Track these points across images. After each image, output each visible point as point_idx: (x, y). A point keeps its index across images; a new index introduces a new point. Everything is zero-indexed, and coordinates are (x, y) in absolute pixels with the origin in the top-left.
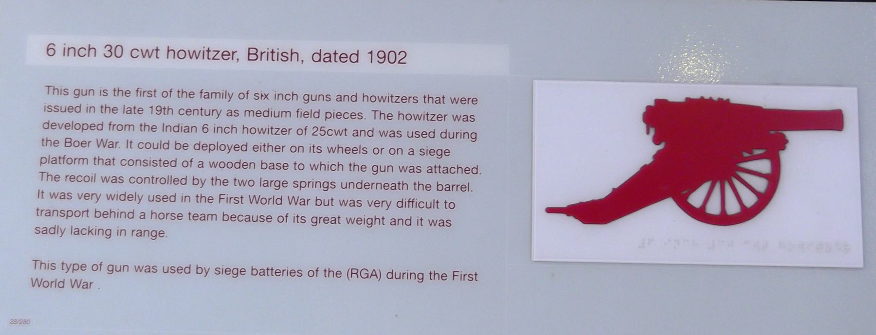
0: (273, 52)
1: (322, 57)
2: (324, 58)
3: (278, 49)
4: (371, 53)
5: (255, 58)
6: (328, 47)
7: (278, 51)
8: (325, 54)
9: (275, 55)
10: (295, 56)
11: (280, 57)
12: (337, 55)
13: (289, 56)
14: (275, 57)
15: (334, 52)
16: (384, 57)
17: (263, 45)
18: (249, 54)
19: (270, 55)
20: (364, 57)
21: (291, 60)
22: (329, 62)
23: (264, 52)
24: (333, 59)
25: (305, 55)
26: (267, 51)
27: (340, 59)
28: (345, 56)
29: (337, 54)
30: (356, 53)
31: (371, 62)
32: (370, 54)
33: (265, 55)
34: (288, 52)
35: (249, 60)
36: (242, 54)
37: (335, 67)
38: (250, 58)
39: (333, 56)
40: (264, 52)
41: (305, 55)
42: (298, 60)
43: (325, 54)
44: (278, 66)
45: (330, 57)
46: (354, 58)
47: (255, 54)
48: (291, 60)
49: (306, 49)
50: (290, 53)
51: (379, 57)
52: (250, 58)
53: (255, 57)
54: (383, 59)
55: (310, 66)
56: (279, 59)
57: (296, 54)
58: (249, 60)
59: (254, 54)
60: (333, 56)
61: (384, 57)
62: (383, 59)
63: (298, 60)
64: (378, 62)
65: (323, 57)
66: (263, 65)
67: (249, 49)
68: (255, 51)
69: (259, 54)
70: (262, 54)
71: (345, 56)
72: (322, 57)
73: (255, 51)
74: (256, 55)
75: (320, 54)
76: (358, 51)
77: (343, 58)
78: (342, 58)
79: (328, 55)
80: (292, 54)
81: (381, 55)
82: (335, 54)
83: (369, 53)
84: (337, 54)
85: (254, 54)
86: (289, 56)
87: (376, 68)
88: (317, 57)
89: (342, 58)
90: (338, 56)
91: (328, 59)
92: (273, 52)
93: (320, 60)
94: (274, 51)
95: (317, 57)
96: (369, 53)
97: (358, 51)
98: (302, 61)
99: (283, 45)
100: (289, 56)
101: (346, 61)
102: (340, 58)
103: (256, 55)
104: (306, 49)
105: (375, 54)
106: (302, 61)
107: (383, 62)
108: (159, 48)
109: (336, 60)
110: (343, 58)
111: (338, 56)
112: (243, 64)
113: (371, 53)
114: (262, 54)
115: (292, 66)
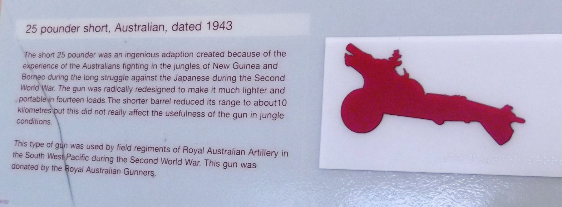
4: (209, 23)
7: (151, 24)
12: (188, 26)
16: (217, 26)
20: (205, 26)
24: (185, 29)
25: (168, 27)
27: (189, 28)
29: (188, 25)
32: (209, 24)
37: (187, 34)
39: (185, 26)
41: (168, 27)
42: (163, 30)
43: (180, 26)
45: (183, 27)
46: (198, 27)
49: (169, 22)
54: (217, 27)
55: (170, 34)
60: (185, 26)
61: (217, 26)
62: (217, 27)
63: (163, 30)
65: (179, 27)
75: (177, 26)
77: (192, 27)
78: (191, 27)
79: (182, 26)
81: (216, 24)
82: (187, 25)
83: (208, 23)
84: (188, 25)
88: (175, 28)
89: (191, 27)
90: (188, 26)
96: (208, 23)
98: (166, 30)
102: (190, 27)
104: (169, 22)
105: (211, 24)
106: (166, 30)
107: (217, 29)
108: (107, 25)
109: (187, 29)
110: (192, 27)
111: (188, 26)
113: (209, 23)
115: (160, 34)
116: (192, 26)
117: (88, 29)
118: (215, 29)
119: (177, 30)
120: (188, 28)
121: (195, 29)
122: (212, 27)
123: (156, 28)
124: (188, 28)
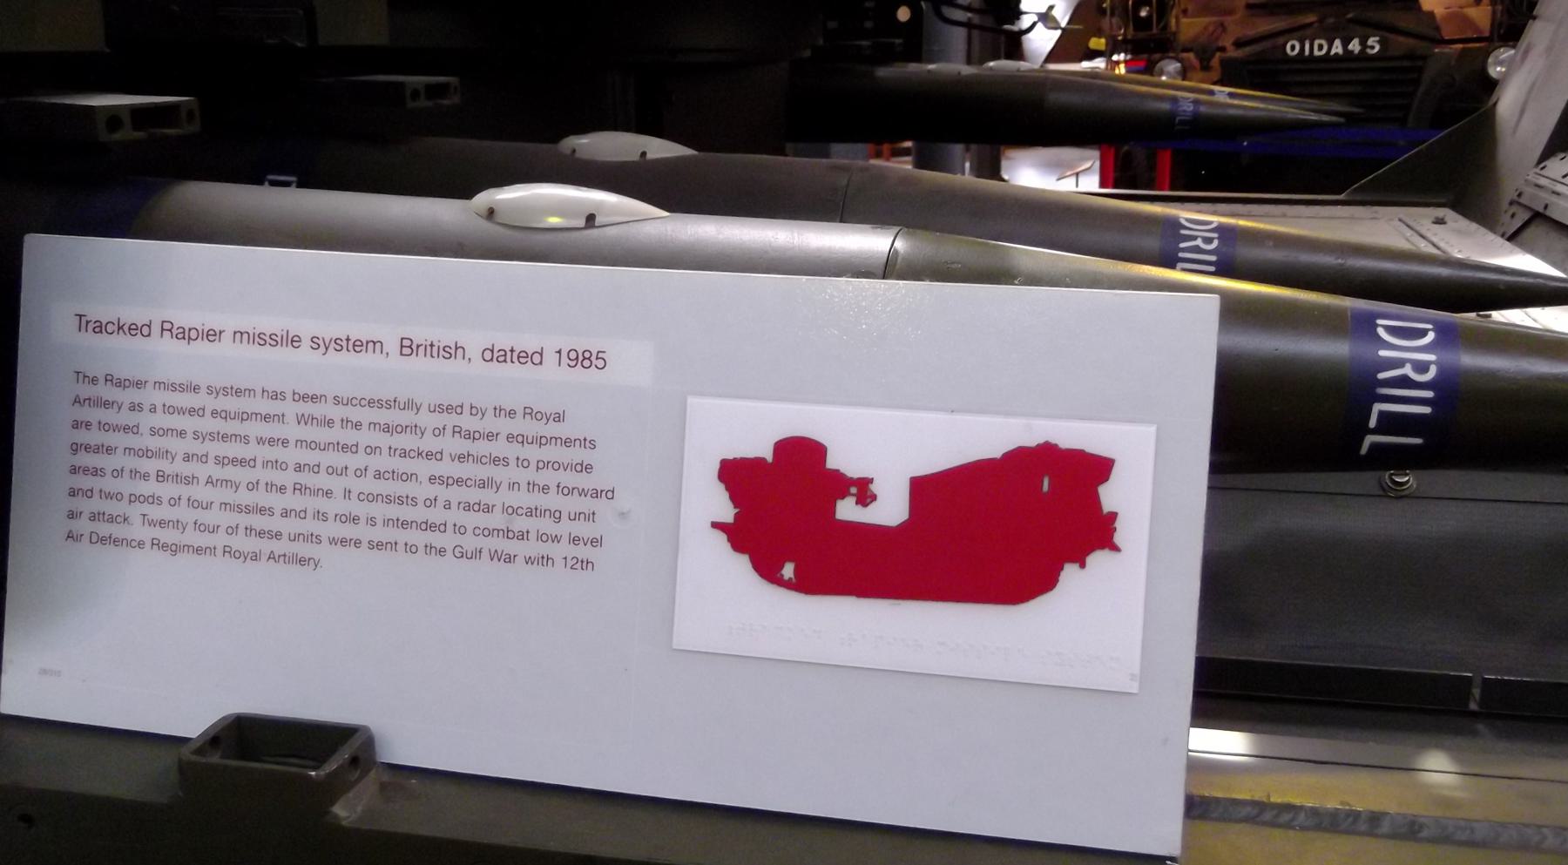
0: (432, 345)
4: (559, 352)
5: (409, 353)
6: (504, 341)
9: (435, 349)
10: (460, 351)
11: (442, 352)
13: (453, 352)
17: (420, 335)
18: (402, 346)
19: (429, 348)
20: (550, 358)
21: (455, 357)
23: (422, 345)
25: (474, 351)
26: (424, 343)
28: (525, 355)
30: (540, 351)
31: (560, 365)
33: (421, 349)
35: (401, 354)
36: (392, 346)
37: (513, 370)
38: (404, 352)
39: (509, 354)
40: (422, 345)
41: (474, 351)
42: (464, 358)
45: (505, 355)
46: (537, 358)
47: (410, 347)
48: (455, 357)
49: (475, 342)
50: (453, 347)
51: (570, 359)
53: (407, 351)
55: (479, 367)
56: (440, 356)
58: (401, 354)
59: (408, 347)
60: (509, 354)
63: (464, 358)
64: (569, 365)
66: (420, 363)
67: (402, 339)
69: (414, 347)
70: (418, 346)
71: (524, 355)
75: (492, 351)
77: (524, 357)
79: (503, 353)
80: (456, 348)
81: (573, 355)
82: (512, 351)
85: (408, 347)
86: (452, 351)
90: (515, 355)
92: (432, 345)
94: (434, 343)
95: (488, 355)
98: (470, 359)
99: (446, 337)
100: (452, 351)
104: (475, 342)
105: (564, 354)
110: (524, 357)
111: (515, 355)
112: (396, 362)
113: (559, 352)
114: (418, 346)
115: (454, 366)
116: (524, 355)
117: (453, 352)
119: (492, 360)
120: (515, 359)
121: (530, 362)
122: (565, 360)
124: (515, 359)
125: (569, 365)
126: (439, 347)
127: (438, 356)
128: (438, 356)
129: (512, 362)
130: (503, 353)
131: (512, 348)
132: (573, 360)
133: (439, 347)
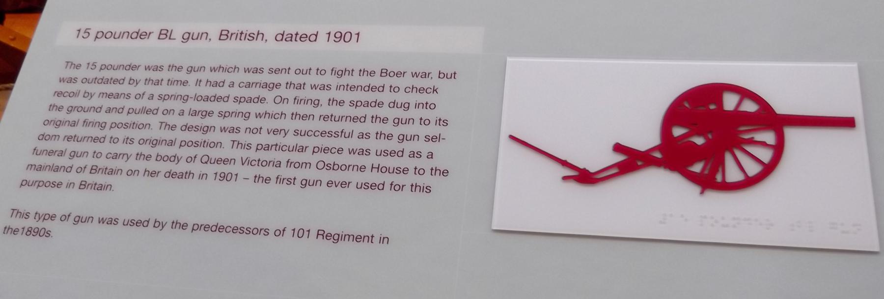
0: (242, 33)
1: (283, 37)
2: (287, 38)
3: (247, 31)
6: (291, 29)
8: (287, 35)
10: (260, 36)
11: (248, 37)
12: (298, 36)
14: (243, 38)
15: (296, 33)
16: (341, 37)
17: (234, 28)
19: (239, 35)
20: (322, 37)
22: (290, 42)
23: (234, 33)
31: (328, 41)
33: (234, 36)
34: (255, 33)
40: (234, 33)
44: (246, 45)
45: (292, 37)
49: (270, 30)
52: (221, 38)
55: (272, 44)
57: (262, 35)
59: (225, 35)
61: (341, 37)
63: (262, 40)
64: (335, 41)
68: (226, 32)
72: (283, 37)
73: (225, 33)
74: (227, 36)
75: (283, 35)
76: (317, 32)
77: (304, 38)
81: (338, 35)
82: (297, 34)
83: (327, 34)
85: (225, 35)
87: (332, 46)
88: (280, 37)
90: (298, 37)
91: (290, 39)
93: (282, 40)
96: (327, 34)
97: (317, 32)
101: (305, 40)
103: (227, 36)
104: (270, 30)
109: (297, 40)
110: (304, 38)
111: (298, 37)
113: (329, 34)
114: (232, 34)
115: (258, 44)
118: (336, 40)
122: (332, 37)
123: (252, 37)
124: (298, 39)
125: (335, 41)
126: (246, 34)
127: (245, 39)
128: (245, 39)
129: (296, 40)
130: (290, 36)
131: (297, 33)
132: (338, 38)
133: (246, 34)
